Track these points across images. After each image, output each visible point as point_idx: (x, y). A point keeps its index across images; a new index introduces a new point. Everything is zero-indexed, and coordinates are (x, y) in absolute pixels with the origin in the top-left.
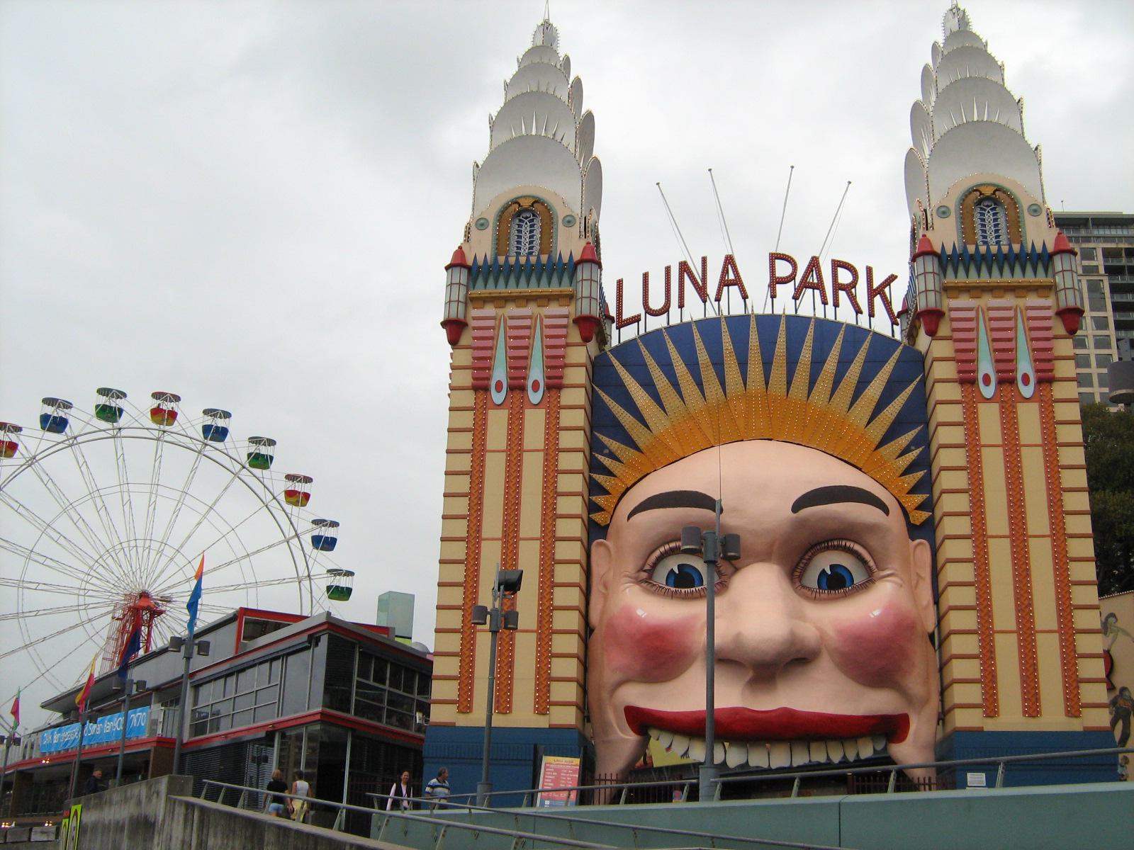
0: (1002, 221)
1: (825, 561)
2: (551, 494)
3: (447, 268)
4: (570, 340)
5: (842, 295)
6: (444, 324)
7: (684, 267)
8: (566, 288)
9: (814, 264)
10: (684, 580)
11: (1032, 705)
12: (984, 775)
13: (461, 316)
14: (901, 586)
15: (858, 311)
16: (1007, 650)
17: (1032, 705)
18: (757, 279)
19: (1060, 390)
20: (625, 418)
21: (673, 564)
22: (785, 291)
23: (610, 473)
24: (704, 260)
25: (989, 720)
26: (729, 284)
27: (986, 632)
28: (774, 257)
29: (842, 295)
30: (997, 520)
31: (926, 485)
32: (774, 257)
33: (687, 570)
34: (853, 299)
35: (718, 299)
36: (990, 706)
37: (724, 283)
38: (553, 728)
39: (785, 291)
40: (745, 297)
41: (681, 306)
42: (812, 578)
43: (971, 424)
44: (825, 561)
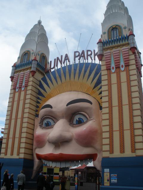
0: (118, 32)
3: (12, 66)
4: (30, 77)
5: (89, 57)
6: (10, 77)
7: (58, 58)
8: (29, 66)
9: (83, 52)
11: (122, 150)
12: (109, 169)
13: (13, 76)
14: (95, 121)
15: (92, 60)
16: (116, 136)
17: (122, 150)
18: (71, 56)
19: (131, 67)
21: (45, 121)
22: (77, 59)
24: (62, 56)
25: (111, 155)
26: (66, 60)
27: (111, 132)
28: (75, 52)
29: (89, 57)
30: (115, 102)
32: (75, 52)
33: (48, 122)
34: (91, 58)
35: (64, 63)
36: (111, 151)
37: (65, 59)
38: (20, 158)
39: (77, 59)
40: (69, 62)
41: (57, 66)
42: (75, 122)
43: (109, 80)
44: (77, 118)
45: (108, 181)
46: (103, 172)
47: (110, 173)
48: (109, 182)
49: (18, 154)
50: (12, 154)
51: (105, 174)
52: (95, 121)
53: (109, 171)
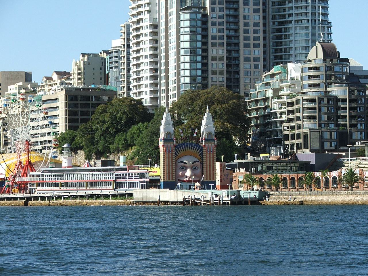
1: (194, 167)
2: (172, 161)
10: (183, 169)
11: (210, 179)
17: (210, 179)
20: (177, 153)
31: (202, 159)
36: (207, 179)
49: (172, 179)
50: (169, 179)
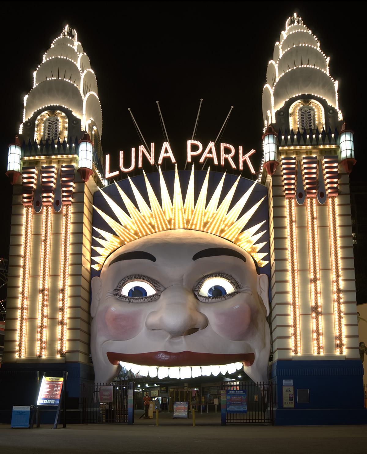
12: (292, 380)
14: (251, 295)
23: (101, 246)
45: (291, 399)
46: (281, 385)
47: (295, 386)
48: (293, 401)
51: (285, 389)
52: (251, 295)
53: (292, 383)
